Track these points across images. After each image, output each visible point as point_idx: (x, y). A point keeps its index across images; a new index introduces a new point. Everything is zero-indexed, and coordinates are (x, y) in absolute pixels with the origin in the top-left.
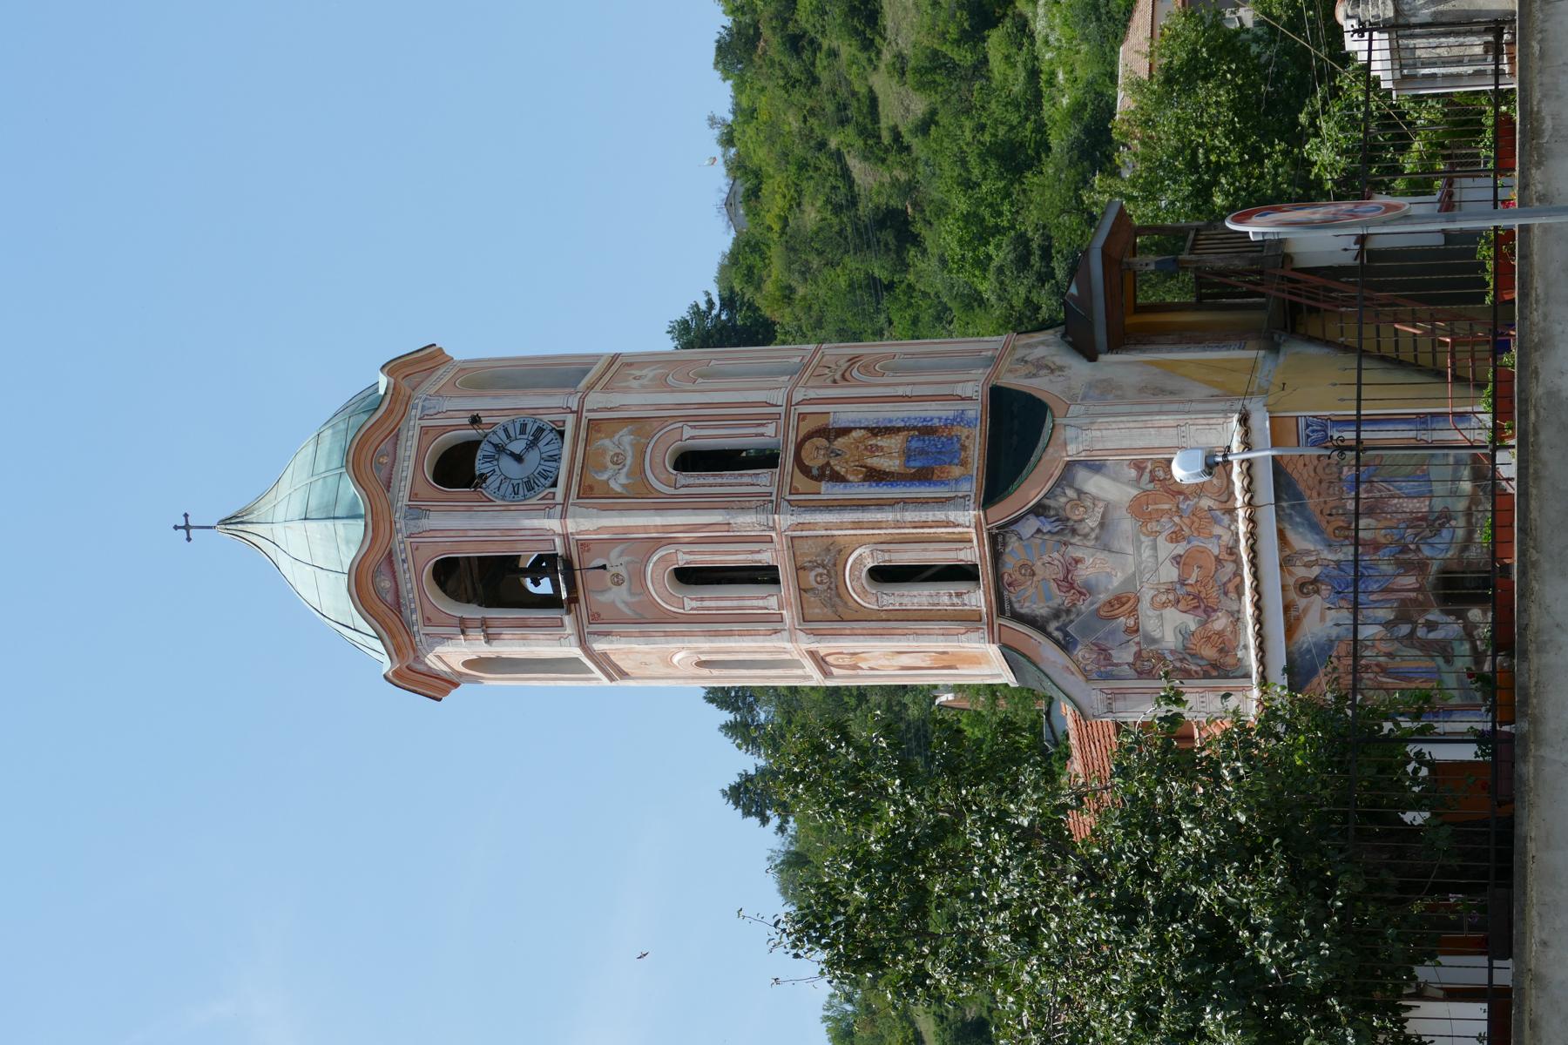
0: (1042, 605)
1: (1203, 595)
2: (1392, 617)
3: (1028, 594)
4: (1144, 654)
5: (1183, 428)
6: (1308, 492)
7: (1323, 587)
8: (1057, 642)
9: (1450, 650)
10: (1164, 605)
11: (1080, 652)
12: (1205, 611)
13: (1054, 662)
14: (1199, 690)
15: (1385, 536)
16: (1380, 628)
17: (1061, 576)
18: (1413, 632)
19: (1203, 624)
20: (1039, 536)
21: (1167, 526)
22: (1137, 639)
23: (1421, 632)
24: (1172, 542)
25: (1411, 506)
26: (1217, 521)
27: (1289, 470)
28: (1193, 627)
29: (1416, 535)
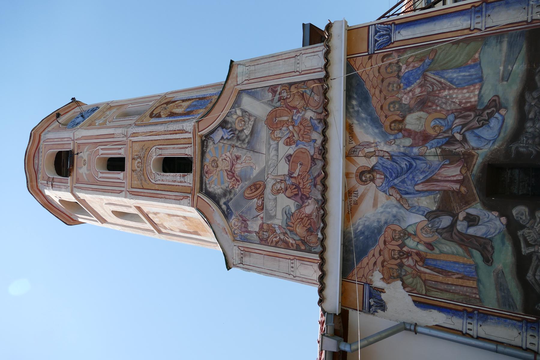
0: (219, 186)
1: (301, 186)
2: (435, 208)
3: (214, 179)
4: (265, 227)
5: (298, 57)
6: (373, 91)
7: (378, 176)
8: (223, 212)
9: (490, 249)
10: (278, 192)
11: (233, 220)
12: (301, 198)
13: (219, 224)
14: (292, 258)
15: (434, 128)
16: (423, 218)
17: (229, 168)
18: (453, 225)
19: (299, 207)
20: (222, 141)
21: (284, 133)
22: (262, 215)
23: (461, 226)
24: (287, 145)
25: (460, 96)
26: (315, 128)
28: (293, 210)
29: (463, 126)
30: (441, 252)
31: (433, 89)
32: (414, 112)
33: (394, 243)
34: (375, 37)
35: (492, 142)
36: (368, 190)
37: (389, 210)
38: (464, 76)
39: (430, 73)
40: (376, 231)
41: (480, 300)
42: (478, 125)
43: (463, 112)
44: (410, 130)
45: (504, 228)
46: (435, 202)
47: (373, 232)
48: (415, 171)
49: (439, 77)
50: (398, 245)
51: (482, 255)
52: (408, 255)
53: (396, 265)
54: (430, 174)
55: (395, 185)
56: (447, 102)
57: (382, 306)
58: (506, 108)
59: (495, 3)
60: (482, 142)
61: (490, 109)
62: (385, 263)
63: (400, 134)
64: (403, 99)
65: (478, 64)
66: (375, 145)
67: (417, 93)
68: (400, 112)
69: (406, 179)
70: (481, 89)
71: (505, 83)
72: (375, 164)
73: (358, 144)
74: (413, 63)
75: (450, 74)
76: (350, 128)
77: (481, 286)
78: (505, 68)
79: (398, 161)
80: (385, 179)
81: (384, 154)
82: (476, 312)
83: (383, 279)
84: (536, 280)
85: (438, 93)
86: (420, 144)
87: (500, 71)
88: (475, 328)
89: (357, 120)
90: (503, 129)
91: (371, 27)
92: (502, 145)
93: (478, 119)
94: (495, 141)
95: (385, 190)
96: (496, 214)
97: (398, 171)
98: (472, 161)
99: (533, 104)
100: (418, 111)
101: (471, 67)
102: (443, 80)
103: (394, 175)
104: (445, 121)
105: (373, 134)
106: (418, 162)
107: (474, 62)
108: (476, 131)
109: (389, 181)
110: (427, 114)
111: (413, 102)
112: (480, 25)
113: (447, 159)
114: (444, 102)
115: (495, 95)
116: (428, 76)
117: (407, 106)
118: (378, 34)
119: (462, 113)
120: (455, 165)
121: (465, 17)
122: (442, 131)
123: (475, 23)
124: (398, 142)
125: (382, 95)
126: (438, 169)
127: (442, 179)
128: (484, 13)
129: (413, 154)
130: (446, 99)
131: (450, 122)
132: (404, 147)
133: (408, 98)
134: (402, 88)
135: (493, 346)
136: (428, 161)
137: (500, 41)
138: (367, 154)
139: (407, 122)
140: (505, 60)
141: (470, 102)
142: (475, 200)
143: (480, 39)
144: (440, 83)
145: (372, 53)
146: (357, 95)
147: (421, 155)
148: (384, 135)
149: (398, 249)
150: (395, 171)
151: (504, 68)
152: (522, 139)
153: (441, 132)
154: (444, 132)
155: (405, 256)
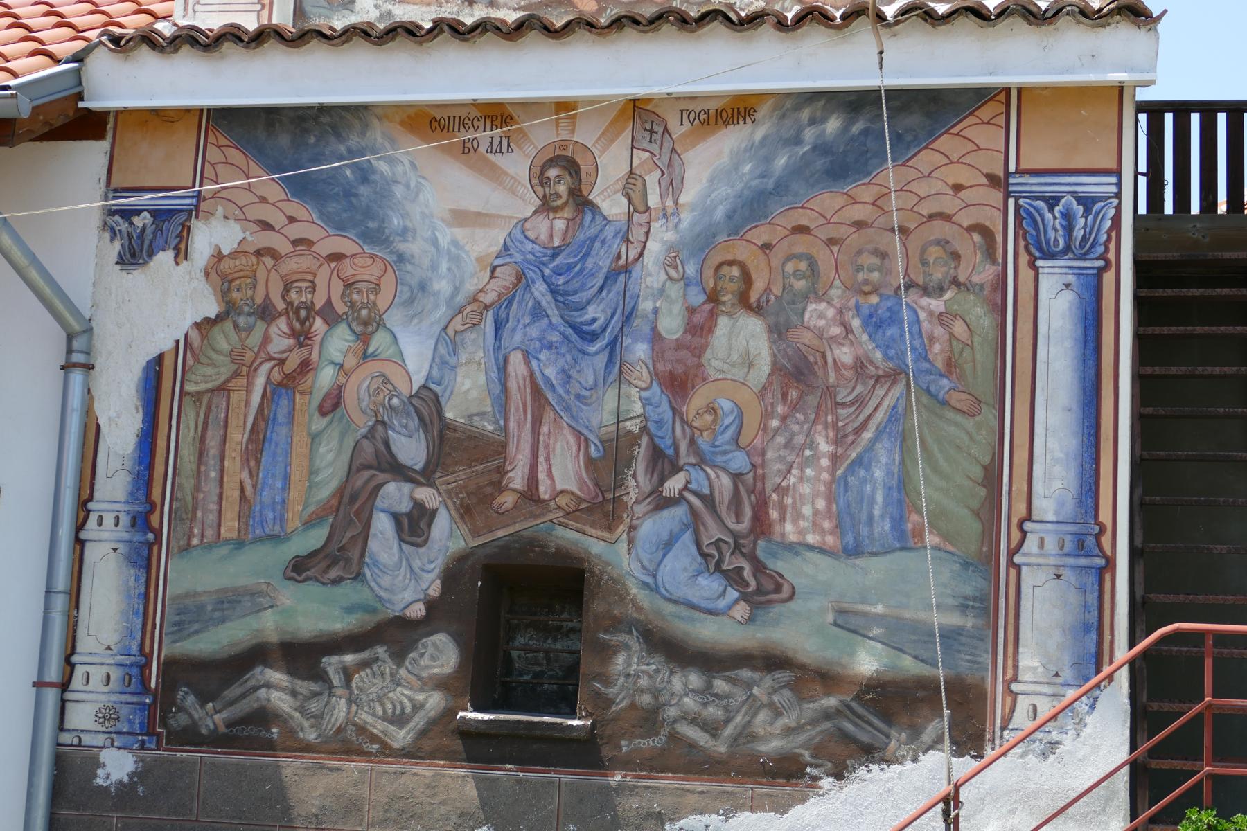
2: (449, 415)
7: (560, 225)
9: (333, 573)
15: (711, 409)
18: (400, 471)
23: (396, 495)
25: (806, 489)
27: (944, 142)
29: (709, 501)
30: (315, 438)
31: (844, 405)
32: (772, 342)
33: (338, 287)
34: (1069, 197)
35: (649, 580)
36: (513, 192)
37: (444, 266)
38: (872, 501)
39: (902, 394)
40: (372, 225)
41: (187, 548)
42: (706, 542)
43: (753, 497)
44: (711, 330)
45: (395, 610)
46: (470, 417)
47: (368, 214)
48: (570, 351)
49: (880, 424)
50: (329, 302)
51: (314, 553)
52: (302, 336)
53: (267, 295)
54: (561, 399)
55: (528, 286)
56: (793, 449)
57: (133, 255)
58: (751, 619)
59: (1096, 595)
60: (652, 553)
61: (755, 576)
62: (268, 261)
63: (702, 298)
64: (823, 305)
65: (905, 540)
66: (670, 211)
67: (837, 352)
68: (776, 297)
69: (545, 320)
70: (821, 550)
71: (830, 618)
72: (601, 213)
73: (676, 147)
74: (947, 336)
75: (884, 459)
76: (739, 112)
77: (224, 550)
78: (879, 619)
79: (609, 292)
80: (549, 252)
81: (635, 244)
82: (151, 536)
83: (218, 256)
84: (256, 688)
85: (826, 422)
86: (660, 367)
87: (871, 604)
88: (105, 535)
89: (764, 138)
90: (685, 612)
91: (1114, 180)
92: (639, 609)
93: (726, 543)
94: (654, 589)
95: (512, 251)
96: (435, 591)
97: (575, 293)
98: (593, 525)
99: (756, 691)
100: (775, 355)
101: (898, 522)
102: (868, 435)
103: (561, 280)
104: (728, 443)
105: (708, 202)
106: (602, 360)
107: (914, 530)
108: (688, 537)
109: (540, 265)
110: (761, 386)
111: (808, 338)
112: (1035, 550)
113: (604, 450)
114: (795, 441)
115: (796, 589)
116: (889, 389)
117: (795, 319)
118: (1080, 210)
119: (749, 498)
120: (584, 475)
121: (1070, 507)
122: (697, 433)
123: (1042, 535)
124: (674, 291)
125: (844, 231)
126: (574, 424)
127: (541, 438)
128: (1071, 561)
129: (627, 341)
130: (804, 446)
131: (724, 458)
132: (656, 311)
133: (822, 323)
134: (861, 300)
135: (61, 582)
136: (600, 393)
137: (967, 607)
138: (639, 183)
139: (740, 322)
140: (903, 619)
141: (783, 519)
142: (475, 533)
143: (985, 549)
144: (863, 427)
145: (1011, 189)
146: (860, 134)
147: (625, 369)
148: (703, 242)
149: (318, 305)
150: (575, 284)
151: (878, 615)
152: (652, 661)
153: (694, 433)
154: (692, 442)
155: (297, 325)
